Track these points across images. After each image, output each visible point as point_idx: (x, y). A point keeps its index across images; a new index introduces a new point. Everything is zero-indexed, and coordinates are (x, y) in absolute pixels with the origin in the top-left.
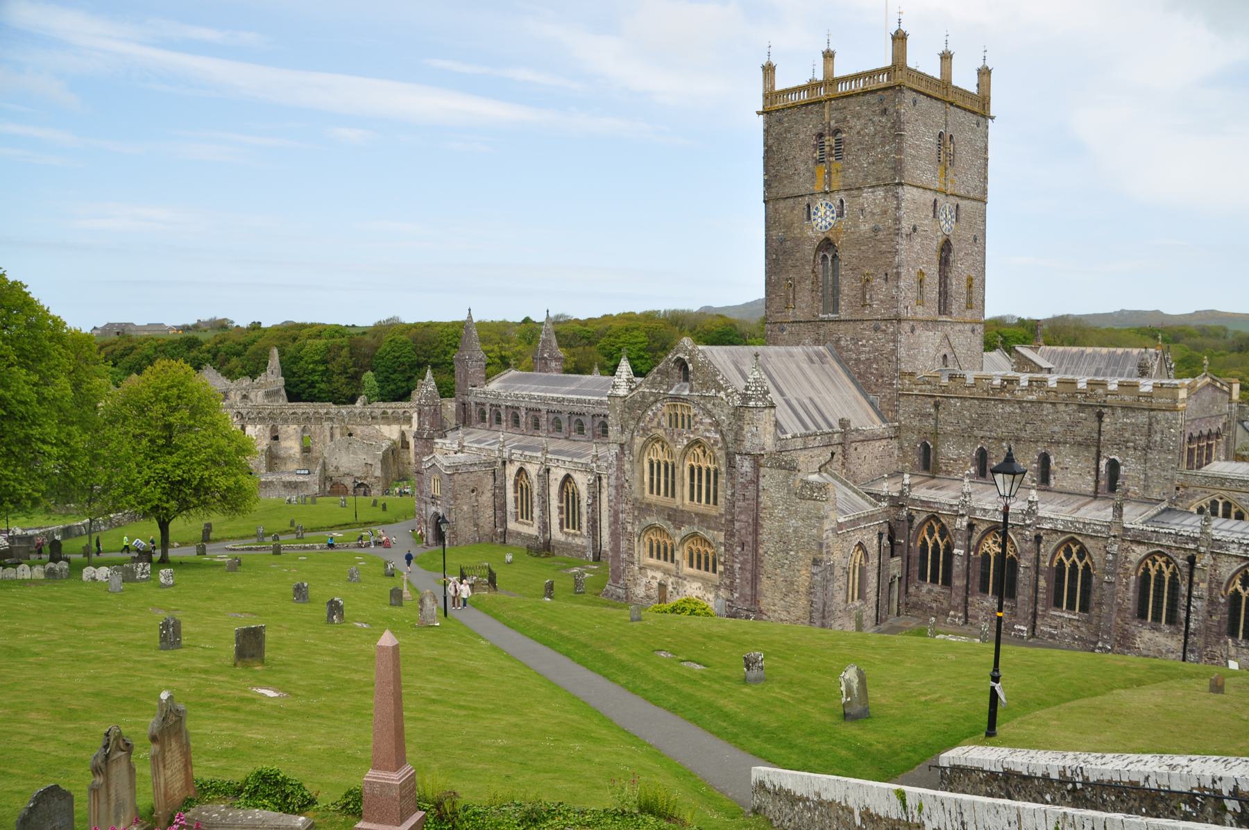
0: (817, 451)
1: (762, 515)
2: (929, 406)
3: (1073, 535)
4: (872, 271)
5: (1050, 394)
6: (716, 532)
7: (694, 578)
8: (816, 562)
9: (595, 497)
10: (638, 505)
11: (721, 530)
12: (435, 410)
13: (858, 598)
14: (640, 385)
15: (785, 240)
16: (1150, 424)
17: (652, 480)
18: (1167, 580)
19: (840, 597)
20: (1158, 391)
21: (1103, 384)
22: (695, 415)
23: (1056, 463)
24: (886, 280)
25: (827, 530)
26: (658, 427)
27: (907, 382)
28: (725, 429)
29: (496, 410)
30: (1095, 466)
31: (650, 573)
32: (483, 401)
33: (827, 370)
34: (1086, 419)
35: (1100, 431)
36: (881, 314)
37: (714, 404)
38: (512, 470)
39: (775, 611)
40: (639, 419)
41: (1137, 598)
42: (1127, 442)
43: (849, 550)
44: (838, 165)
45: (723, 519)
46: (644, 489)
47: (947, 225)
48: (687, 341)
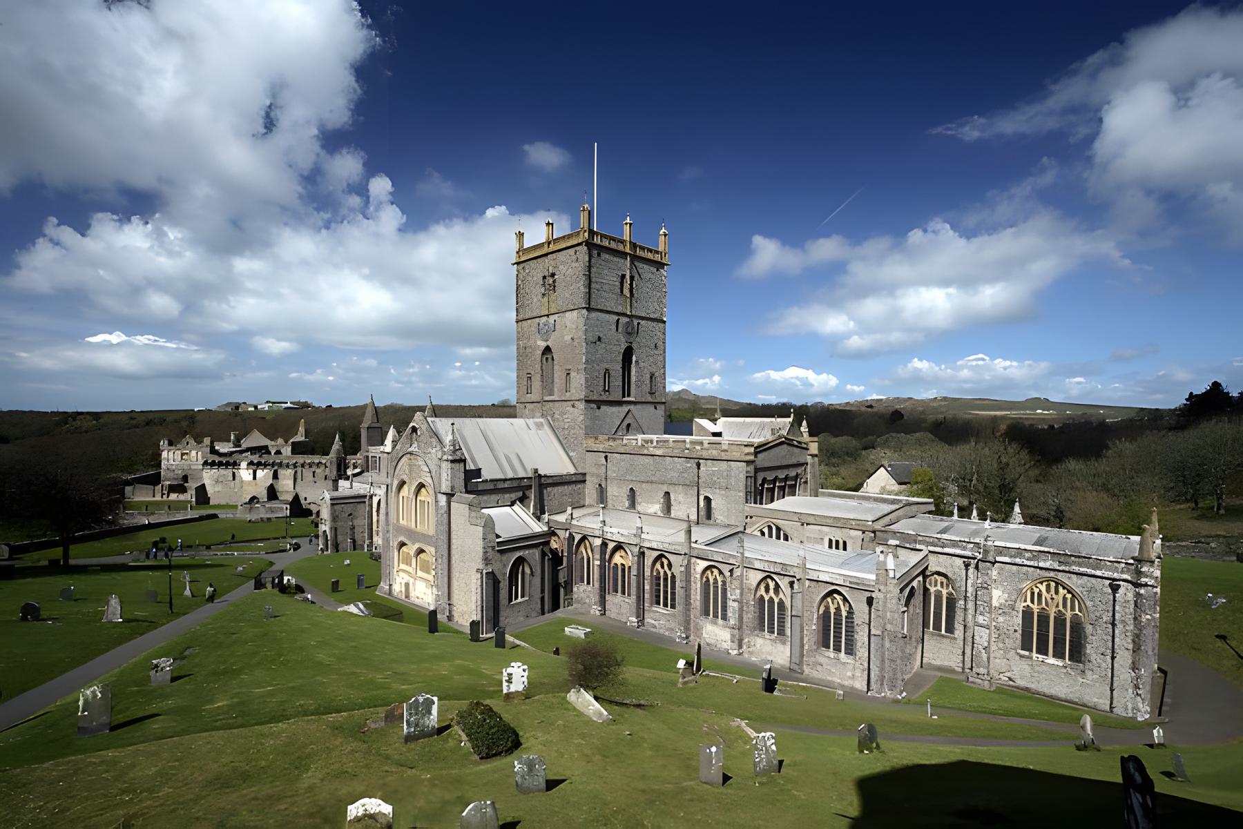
20: (733, 447)
23: (675, 500)
31: (401, 574)
35: (698, 476)
44: (553, 297)
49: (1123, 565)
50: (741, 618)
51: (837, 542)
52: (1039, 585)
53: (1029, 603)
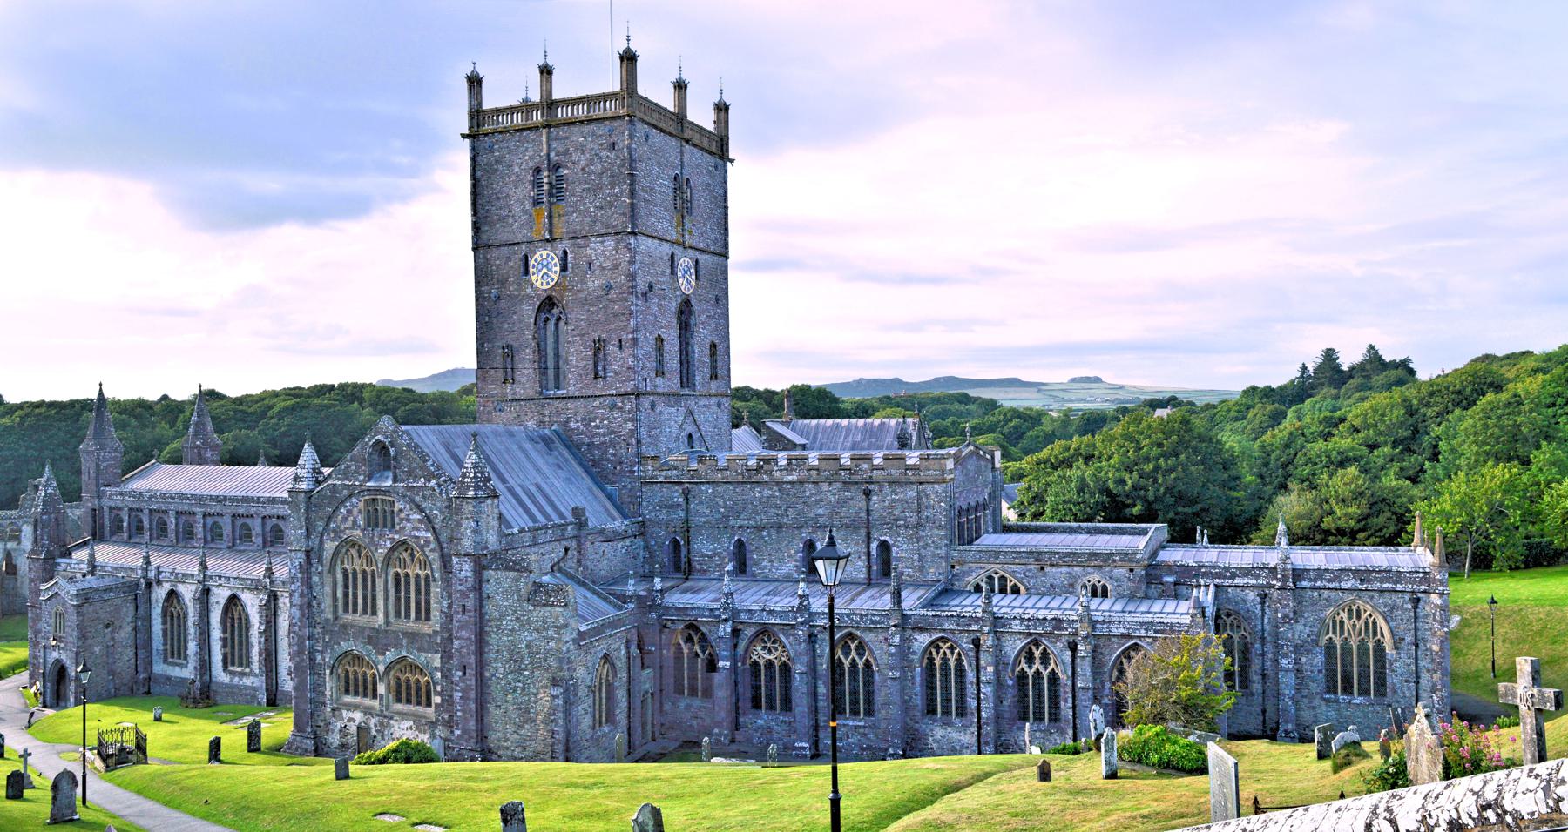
0: (548, 548)
1: (487, 629)
2: (676, 495)
3: (850, 629)
5: (812, 472)
6: (430, 655)
7: (404, 716)
8: (555, 682)
9: (268, 622)
10: (329, 628)
11: (436, 652)
12: (56, 519)
13: (607, 721)
14: (330, 475)
16: (919, 499)
17: (346, 595)
18: (952, 668)
19: (586, 722)
21: (869, 458)
22: (401, 510)
24: (621, 347)
25: (567, 642)
26: (351, 529)
27: (650, 468)
29: (136, 516)
30: (865, 550)
32: (120, 504)
34: (852, 499)
36: (616, 388)
37: (424, 496)
38: (160, 593)
39: (508, 748)
40: (329, 519)
45: (439, 638)
46: (335, 607)
47: (687, 285)
48: (386, 422)
49: (1421, 575)
52: (1341, 612)
53: (1331, 635)
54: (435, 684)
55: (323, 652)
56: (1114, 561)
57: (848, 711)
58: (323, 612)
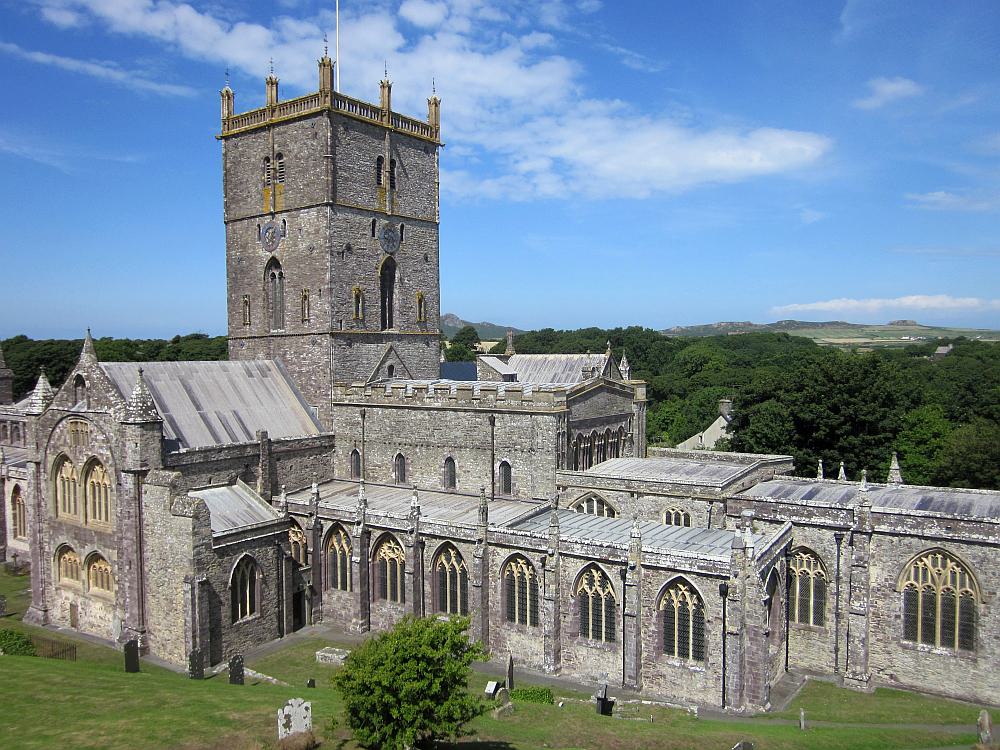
1: (145, 532)
4: (309, 287)
10: (52, 524)
11: (114, 549)
15: (241, 260)
17: (64, 496)
27: (339, 392)
28: (113, 446)
31: (64, 594)
33: (266, 382)
35: (493, 434)
38: (9, 487)
39: (160, 631)
40: (50, 436)
41: (505, 601)
42: (515, 444)
43: (233, 565)
44: (281, 186)
50: (557, 622)
51: (677, 514)
52: (924, 559)
54: (114, 575)
55: (49, 543)
56: (695, 493)
57: (459, 611)
58: (47, 512)
